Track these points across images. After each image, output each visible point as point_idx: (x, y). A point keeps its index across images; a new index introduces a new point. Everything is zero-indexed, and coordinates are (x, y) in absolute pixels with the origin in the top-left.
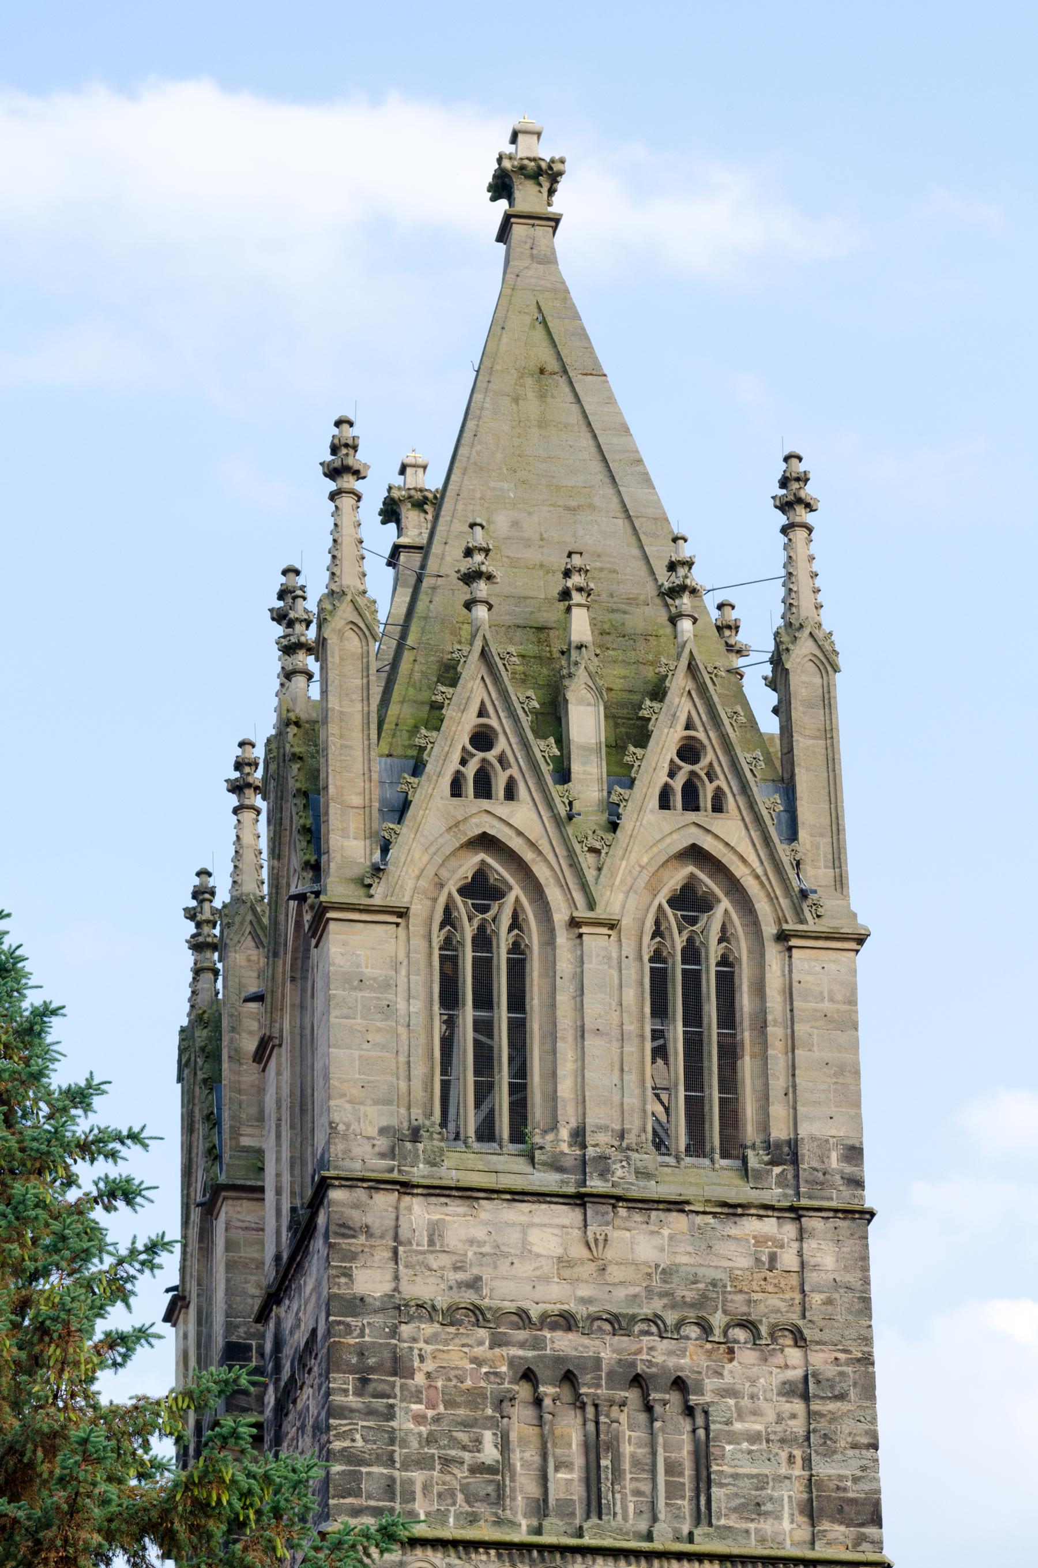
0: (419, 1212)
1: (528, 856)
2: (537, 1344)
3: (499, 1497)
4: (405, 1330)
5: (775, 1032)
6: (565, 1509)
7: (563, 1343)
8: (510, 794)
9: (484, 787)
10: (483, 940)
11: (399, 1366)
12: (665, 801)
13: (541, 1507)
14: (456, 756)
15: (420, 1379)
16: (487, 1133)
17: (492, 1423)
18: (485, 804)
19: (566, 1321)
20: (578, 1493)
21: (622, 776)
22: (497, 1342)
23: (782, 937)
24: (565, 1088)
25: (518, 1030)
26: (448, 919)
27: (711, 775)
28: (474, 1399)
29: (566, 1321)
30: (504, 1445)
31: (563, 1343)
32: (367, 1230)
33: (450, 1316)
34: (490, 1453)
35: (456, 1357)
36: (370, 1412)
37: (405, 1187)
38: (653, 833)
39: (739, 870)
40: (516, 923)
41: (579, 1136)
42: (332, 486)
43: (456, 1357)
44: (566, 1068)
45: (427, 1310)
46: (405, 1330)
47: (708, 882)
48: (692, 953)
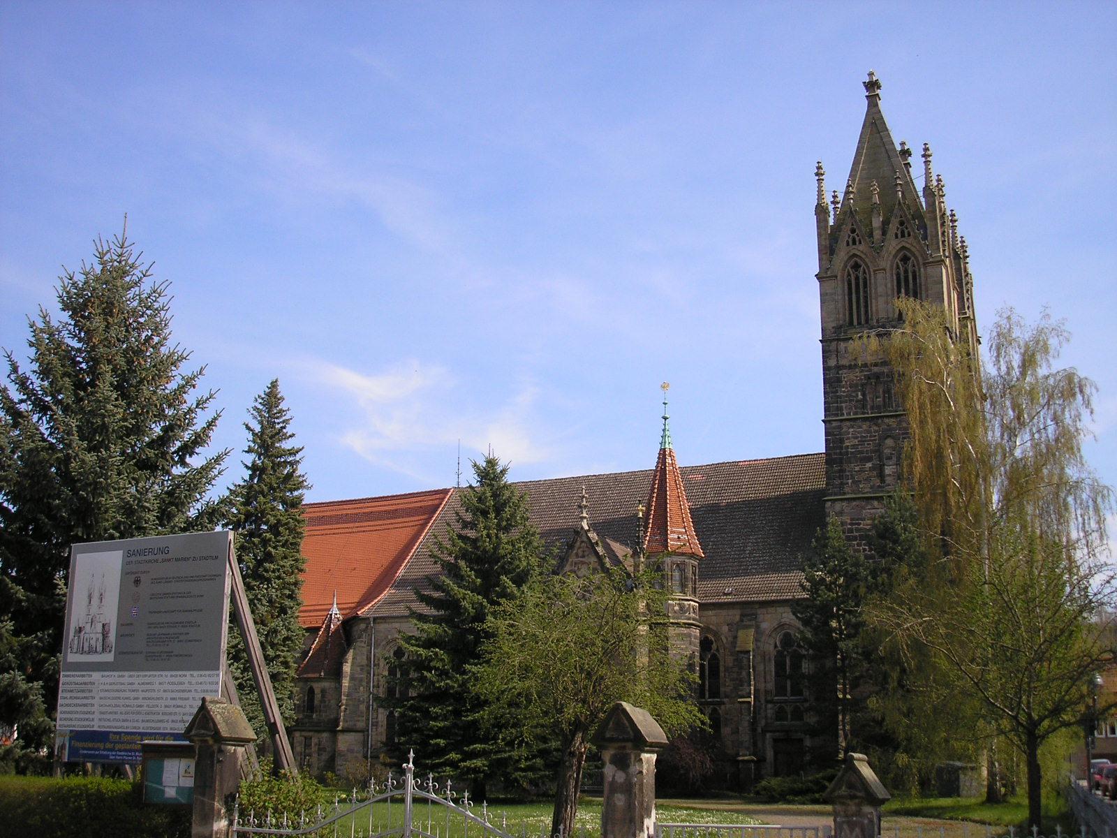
0: (842, 345)
1: (863, 256)
2: (870, 370)
3: (864, 407)
4: (840, 372)
5: (923, 287)
6: (878, 407)
7: (876, 369)
8: (860, 243)
9: (854, 243)
10: (857, 278)
11: (839, 380)
12: (897, 237)
13: (872, 408)
14: (847, 237)
15: (844, 383)
16: (859, 323)
17: (859, 390)
18: (854, 247)
19: (876, 365)
20: (882, 403)
21: (884, 233)
22: (862, 371)
23: (924, 264)
24: (874, 309)
25: (866, 297)
26: (849, 275)
27: (907, 228)
28: (856, 385)
29: (876, 365)
30: (864, 395)
31: (876, 369)
32: (830, 351)
33: (850, 367)
34: (860, 397)
35: (852, 376)
36: (832, 392)
37: (838, 340)
38: (893, 245)
39: (913, 249)
40: (864, 272)
41: (878, 321)
42: (817, 178)
43: (852, 376)
44: (874, 305)
45: (844, 367)
46: (840, 372)
47: (908, 254)
48: (906, 271)
